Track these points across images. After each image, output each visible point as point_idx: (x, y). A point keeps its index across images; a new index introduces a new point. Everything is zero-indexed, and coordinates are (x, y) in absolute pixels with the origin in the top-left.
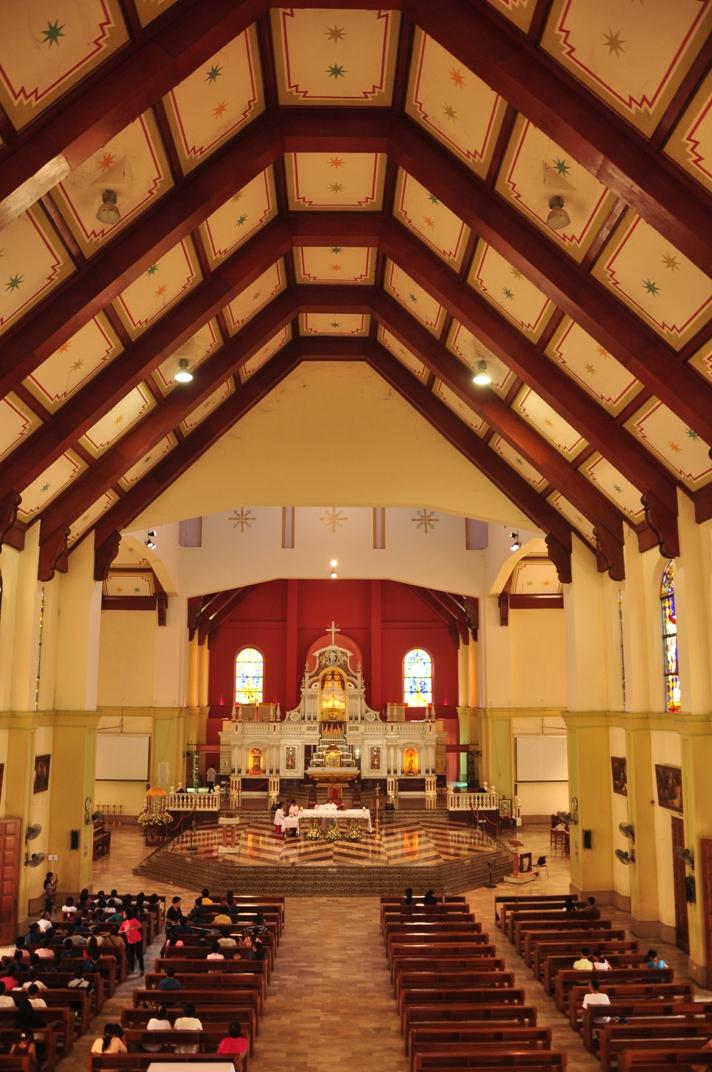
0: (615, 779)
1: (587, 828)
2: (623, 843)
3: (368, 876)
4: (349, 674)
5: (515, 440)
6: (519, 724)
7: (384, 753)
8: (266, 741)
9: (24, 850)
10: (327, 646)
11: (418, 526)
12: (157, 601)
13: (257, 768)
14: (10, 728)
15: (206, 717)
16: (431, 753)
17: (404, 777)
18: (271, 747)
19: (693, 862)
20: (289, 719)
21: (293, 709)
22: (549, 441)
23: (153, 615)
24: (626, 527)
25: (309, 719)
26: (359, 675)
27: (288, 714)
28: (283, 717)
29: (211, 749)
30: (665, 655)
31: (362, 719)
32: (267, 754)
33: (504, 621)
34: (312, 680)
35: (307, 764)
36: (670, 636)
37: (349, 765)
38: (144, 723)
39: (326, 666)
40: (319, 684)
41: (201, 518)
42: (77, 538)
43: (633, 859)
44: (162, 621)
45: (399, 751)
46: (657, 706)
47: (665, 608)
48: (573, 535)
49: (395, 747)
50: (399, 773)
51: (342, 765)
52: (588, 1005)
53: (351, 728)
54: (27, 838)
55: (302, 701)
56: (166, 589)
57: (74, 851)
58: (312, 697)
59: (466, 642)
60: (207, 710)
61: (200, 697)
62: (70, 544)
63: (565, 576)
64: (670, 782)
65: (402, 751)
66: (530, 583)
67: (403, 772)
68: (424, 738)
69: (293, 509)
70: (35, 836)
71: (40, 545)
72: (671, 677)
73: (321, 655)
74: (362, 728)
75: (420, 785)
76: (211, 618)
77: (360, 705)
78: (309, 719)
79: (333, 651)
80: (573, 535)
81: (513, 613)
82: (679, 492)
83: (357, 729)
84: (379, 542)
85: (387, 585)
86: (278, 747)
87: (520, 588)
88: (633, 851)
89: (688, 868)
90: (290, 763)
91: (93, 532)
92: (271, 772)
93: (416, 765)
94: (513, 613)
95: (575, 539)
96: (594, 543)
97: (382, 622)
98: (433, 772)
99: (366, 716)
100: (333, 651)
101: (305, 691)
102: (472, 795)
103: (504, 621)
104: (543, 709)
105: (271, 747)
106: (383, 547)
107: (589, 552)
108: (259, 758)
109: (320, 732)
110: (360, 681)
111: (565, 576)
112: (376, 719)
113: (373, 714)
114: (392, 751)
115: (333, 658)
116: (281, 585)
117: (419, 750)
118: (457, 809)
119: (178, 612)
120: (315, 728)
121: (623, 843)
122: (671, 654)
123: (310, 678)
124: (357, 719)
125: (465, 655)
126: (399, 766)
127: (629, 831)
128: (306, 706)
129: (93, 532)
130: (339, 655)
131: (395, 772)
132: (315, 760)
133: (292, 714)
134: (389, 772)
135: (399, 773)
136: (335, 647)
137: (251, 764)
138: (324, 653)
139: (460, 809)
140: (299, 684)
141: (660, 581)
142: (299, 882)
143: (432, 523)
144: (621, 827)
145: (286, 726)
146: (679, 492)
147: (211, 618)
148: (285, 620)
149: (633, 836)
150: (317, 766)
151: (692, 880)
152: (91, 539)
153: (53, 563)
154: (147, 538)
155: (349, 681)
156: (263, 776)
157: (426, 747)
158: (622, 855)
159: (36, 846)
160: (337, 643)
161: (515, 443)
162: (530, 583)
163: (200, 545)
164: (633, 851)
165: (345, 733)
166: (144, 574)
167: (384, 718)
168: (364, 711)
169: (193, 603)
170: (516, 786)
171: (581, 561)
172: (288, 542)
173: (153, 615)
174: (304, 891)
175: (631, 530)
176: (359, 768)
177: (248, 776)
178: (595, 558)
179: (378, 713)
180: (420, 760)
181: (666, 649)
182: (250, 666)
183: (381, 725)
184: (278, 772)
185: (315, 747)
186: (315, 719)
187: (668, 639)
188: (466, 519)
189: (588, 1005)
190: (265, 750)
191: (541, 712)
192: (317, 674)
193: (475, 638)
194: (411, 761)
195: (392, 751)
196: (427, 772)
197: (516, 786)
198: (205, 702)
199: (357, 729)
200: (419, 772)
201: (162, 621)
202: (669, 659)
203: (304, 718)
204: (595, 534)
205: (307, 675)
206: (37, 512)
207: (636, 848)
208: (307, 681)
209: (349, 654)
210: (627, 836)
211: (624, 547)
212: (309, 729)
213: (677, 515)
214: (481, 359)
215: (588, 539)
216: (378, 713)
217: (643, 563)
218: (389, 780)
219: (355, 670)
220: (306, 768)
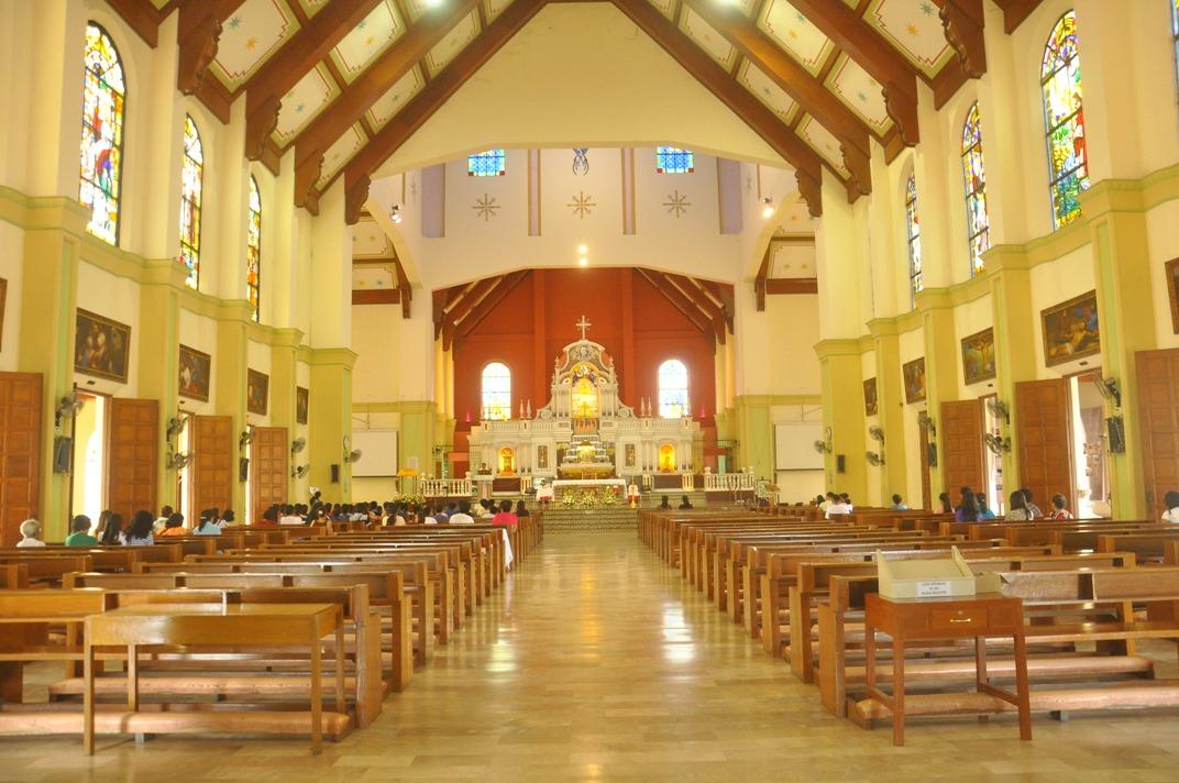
0: (867, 403)
1: (841, 454)
2: (874, 446)
3: (624, 516)
4: (600, 368)
5: (760, 57)
6: (779, 413)
7: (639, 449)
8: (517, 441)
9: (290, 465)
10: (577, 340)
11: (670, 211)
12: (400, 294)
13: (508, 469)
14: (272, 345)
15: (452, 430)
16: (688, 448)
17: (660, 473)
18: (523, 445)
19: (934, 429)
20: (540, 417)
21: (543, 406)
23: (398, 308)
24: (872, 141)
25: (561, 415)
26: (611, 370)
27: (538, 411)
28: (533, 415)
29: (460, 457)
31: (616, 414)
32: (518, 453)
33: (761, 306)
34: (565, 374)
35: (560, 461)
37: (602, 461)
38: (392, 419)
39: (577, 361)
40: (570, 380)
41: (444, 165)
42: (328, 179)
43: (883, 461)
44: (407, 314)
45: (655, 449)
47: (910, 213)
48: (823, 168)
49: (651, 443)
50: (655, 470)
51: (594, 460)
52: (830, 515)
53: (605, 424)
54: (293, 450)
55: (553, 398)
56: (410, 279)
57: (335, 485)
58: (563, 393)
59: (723, 342)
60: (454, 423)
61: (446, 407)
62: (320, 185)
64: (916, 374)
65: (657, 446)
66: (787, 267)
67: (659, 469)
68: (680, 433)
69: (539, 151)
70: (300, 449)
71: (296, 170)
74: (616, 424)
75: (676, 481)
76: (456, 323)
77: (613, 401)
78: (561, 415)
79: (584, 350)
80: (823, 168)
81: (769, 299)
82: (919, 81)
83: (610, 424)
84: (629, 227)
85: (637, 274)
86: (530, 445)
87: (778, 272)
88: (883, 456)
89: (930, 434)
90: (542, 461)
91: (343, 175)
92: (523, 471)
93: (672, 463)
94: (769, 299)
96: (846, 174)
97: (635, 331)
98: (691, 467)
100: (584, 350)
101: (555, 388)
102: (730, 475)
103: (761, 306)
104: (802, 397)
105: (523, 445)
106: (634, 233)
108: (510, 458)
109: (573, 428)
110: (612, 376)
111: (816, 210)
113: (627, 410)
114: (647, 446)
115: (584, 353)
116: (528, 274)
117: (676, 445)
118: (714, 489)
119: (423, 305)
120: (566, 425)
121: (874, 446)
122: (917, 254)
124: (610, 414)
125: (723, 358)
126: (655, 462)
127: (879, 434)
128: (557, 402)
129: (343, 175)
131: (651, 468)
132: (568, 457)
133: (544, 411)
134: (644, 469)
135: (655, 470)
136: (586, 342)
137: (502, 466)
138: (574, 348)
139: (718, 489)
140: (549, 381)
141: (905, 188)
142: (557, 522)
143: (684, 207)
144: (871, 431)
145: (537, 423)
146: (919, 81)
147: (456, 323)
148: (533, 332)
149: (883, 438)
150: (570, 462)
151: (934, 446)
152: (341, 183)
153: (309, 198)
154: (391, 211)
155: (601, 376)
156: (514, 476)
157: (683, 442)
158: (873, 458)
159: (301, 459)
160: (586, 338)
162: (787, 267)
163: (443, 235)
164: (882, 453)
165: (598, 428)
166: (387, 265)
167: (638, 414)
168: (617, 407)
169: (442, 297)
170: (775, 475)
171: (830, 195)
172: (535, 229)
173: (398, 308)
174: (561, 529)
176: (614, 464)
177: (499, 476)
178: (845, 190)
179: (632, 409)
180: (676, 459)
181: (912, 252)
182: (496, 381)
183: (635, 420)
184: (530, 470)
186: (567, 415)
188: (718, 159)
189: (830, 515)
190: (516, 449)
191: (800, 399)
192: (568, 369)
193: (732, 331)
194: (668, 458)
195: (647, 446)
196: (684, 468)
197: (775, 475)
198: (451, 415)
200: (676, 469)
201: (407, 314)
203: (555, 415)
204: (842, 150)
205: (557, 371)
206: (292, 137)
207: (885, 449)
208: (557, 377)
209: (601, 348)
210: (877, 438)
211: (871, 161)
212: (561, 425)
213: (917, 103)
215: (838, 170)
216: (632, 409)
217: (886, 175)
218: (645, 476)
219: (607, 365)
220: (559, 465)
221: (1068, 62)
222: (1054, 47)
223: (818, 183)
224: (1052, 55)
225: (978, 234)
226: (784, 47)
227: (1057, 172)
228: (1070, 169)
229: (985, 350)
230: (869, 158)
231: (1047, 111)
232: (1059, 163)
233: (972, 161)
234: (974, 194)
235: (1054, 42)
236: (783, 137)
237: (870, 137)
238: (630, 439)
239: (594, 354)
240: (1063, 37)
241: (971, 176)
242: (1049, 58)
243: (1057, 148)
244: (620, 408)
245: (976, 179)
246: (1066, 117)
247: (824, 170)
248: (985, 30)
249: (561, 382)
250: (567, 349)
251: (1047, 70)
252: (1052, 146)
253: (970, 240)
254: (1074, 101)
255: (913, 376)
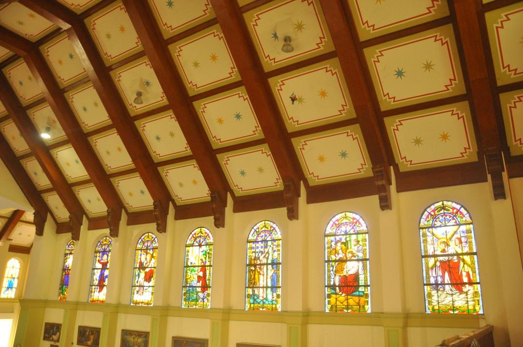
22: (62, 171)
30: (92, 277)
36: (97, 269)
46: (83, 299)
47: (96, 256)
63: (40, 232)
64: (87, 333)
72: (94, 287)
95: (49, 216)
107: (54, 224)
146: (123, 211)
161: (45, 167)
175: (87, 220)
187: (96, 270)
202: (95, 279)
211: (82, 226)
213: (120, 220)
214: (49, 126)
221: (200, 246)
222: (194, 236)
223: (44, 221)
224: (193, 239)
225: (137, 286)
226: (59, 166)
227: (187, 283)
228: (194, 285)
229: (136, 339)
230: (82, 225)
231: (186, 258)
232: (188, 280)
233: (141, 255)
234: (139, 268)
235: (195, 234)
236: (34, 195)
237: (84, 216)
240: (199, 235)
241: (139, 261)
242: (191, 238)
243: (189, 274)
245: (141, 264)
246: (194, 265)
247: (49, 216)
248: (168, 216)
251: (189, 242)
252: (186, 272)
253: (133, 286)
254: (200, 261)
255: (85, 334)
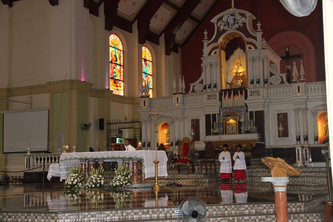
20: (193, 91)
28: (187, 90)
31: (266, 82)
39: (224, 31)
73: (219, 20)
74: (263, 91)
83: (258, 93)
99: (270, 80)
112: (282, 82)
114: (300, 113)
115: (231, 21)
123: (208, 45)
124: (258, 82)
130: (238, 17)
131: (306, 139)
133: (197, 85)
134: (298, 139)
138: (221, 18)
145: (190, 98)
165: (246, 97)
185: (214, 115)
186: (215, 86)
192: (216, 40)
195: (300, 113)
199: (258, 93)
212: (209, 97)
238: (282, 109)
239: (241, 20)
244: (271, 74)
249: (210, 54)
250: (214, 20)
